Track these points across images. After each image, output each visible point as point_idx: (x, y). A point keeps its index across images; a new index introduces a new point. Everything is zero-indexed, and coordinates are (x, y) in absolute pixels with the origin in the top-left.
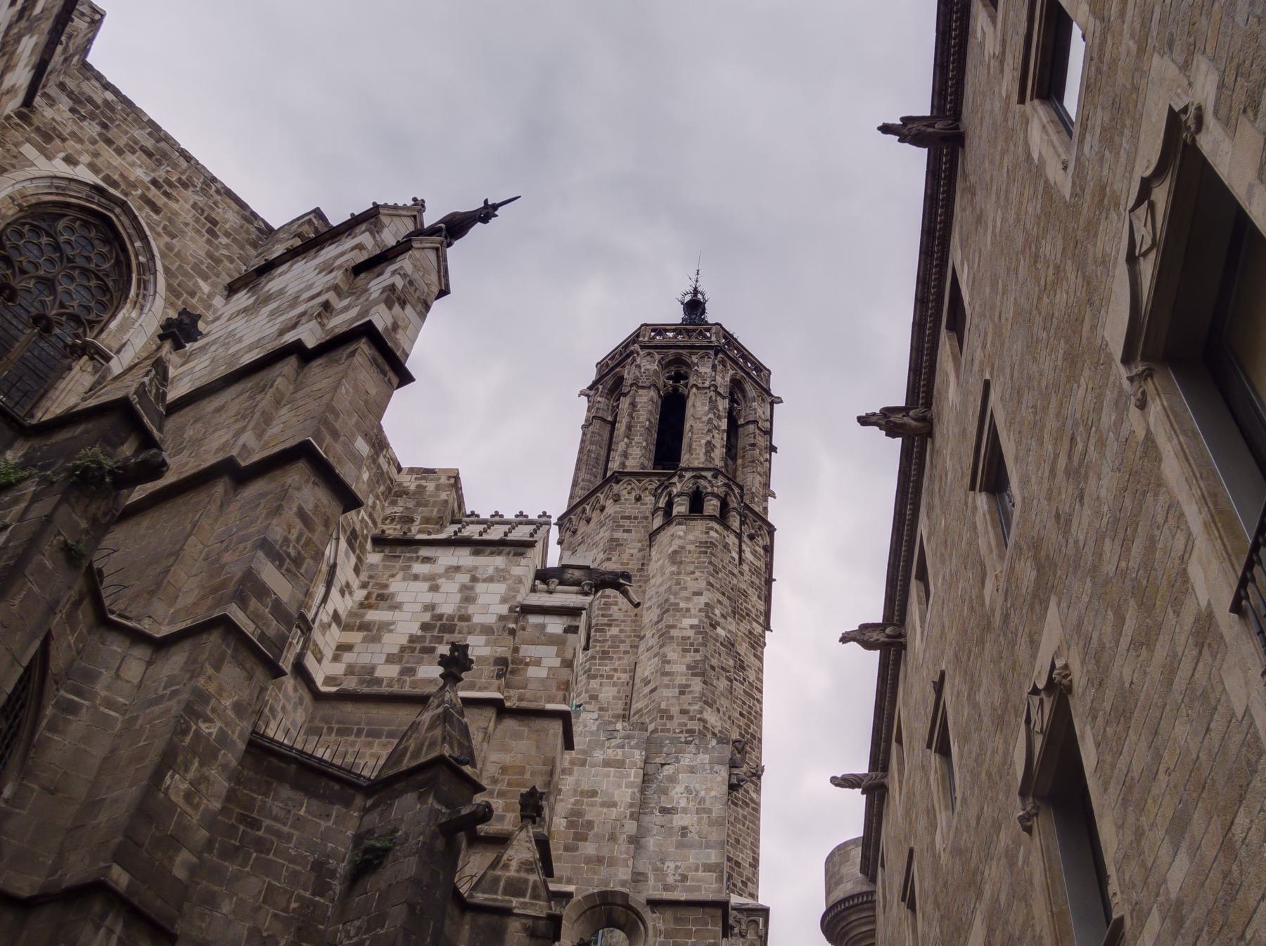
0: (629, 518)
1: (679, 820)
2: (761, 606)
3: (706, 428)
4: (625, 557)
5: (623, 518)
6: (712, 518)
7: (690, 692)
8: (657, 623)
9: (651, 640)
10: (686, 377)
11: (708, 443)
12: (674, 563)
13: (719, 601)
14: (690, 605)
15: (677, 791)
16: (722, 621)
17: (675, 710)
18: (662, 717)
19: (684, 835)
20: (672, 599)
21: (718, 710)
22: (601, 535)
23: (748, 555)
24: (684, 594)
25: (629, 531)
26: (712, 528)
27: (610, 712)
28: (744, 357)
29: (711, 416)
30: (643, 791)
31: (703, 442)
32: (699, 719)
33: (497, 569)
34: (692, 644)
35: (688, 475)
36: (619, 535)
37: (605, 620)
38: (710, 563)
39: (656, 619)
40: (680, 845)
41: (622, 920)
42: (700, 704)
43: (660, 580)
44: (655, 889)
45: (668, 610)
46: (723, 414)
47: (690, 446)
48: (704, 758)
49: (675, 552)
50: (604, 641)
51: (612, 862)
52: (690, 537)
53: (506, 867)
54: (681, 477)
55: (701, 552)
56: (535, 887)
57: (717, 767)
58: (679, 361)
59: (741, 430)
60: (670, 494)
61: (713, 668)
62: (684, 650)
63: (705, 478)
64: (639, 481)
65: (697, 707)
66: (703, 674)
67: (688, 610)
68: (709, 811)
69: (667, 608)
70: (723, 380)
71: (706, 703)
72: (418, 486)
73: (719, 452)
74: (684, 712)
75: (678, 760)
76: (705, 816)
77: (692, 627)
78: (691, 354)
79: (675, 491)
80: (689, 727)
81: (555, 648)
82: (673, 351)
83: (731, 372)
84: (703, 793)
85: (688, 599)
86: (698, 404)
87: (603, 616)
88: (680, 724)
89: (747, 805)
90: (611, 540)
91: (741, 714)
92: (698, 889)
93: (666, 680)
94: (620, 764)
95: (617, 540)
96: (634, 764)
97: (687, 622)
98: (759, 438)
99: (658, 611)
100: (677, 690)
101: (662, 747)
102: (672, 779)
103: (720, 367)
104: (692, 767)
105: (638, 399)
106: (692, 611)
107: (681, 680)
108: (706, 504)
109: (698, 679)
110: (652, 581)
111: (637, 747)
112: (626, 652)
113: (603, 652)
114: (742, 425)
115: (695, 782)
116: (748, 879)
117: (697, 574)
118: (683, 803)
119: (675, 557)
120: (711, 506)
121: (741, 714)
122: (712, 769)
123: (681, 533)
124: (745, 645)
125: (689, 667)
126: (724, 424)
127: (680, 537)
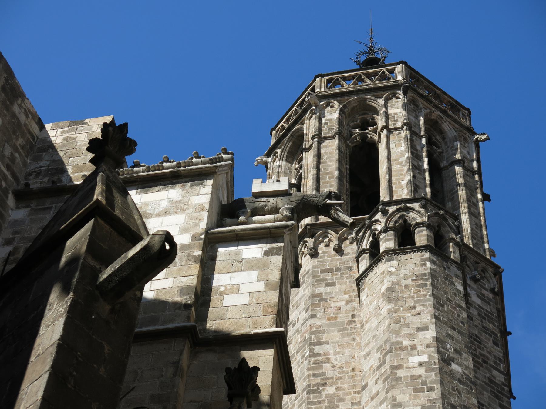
0: (330, 271)
2: (498, 352)
4: (331, 312)
5: (323, 271)
12: (390, 300)
13: (448, 336)
14: (416, 342)
16: (456, 356)
20: (394, 339)
22: (300, 295)
23: (475, 299)
24: (406, 331)
25: (332, 284)
28: (437, 97)
33: (171, 201)
34: (424, 383)
35: (391, 209)
36: (321, 289)
37: (318, 380)
39: (376, 364)
45: (390, 351)
49: (389, 290)
50: (319, 402)
52: (404, 272)
55: (418, 286)
62: (416, 390)
63: (413, 209)
67: (413, 347)
72: (65, 139)
77: (421, 364)
79: (379, 227)
81: (254, 274)
83: (424, 111)
85: (411, 337)
87: (314, 375)
90: (313, 296)
95: (320, 295)
99: (379, 355)
105: (322, 151)
106: (419, 348)
110: (367, 327)
114: (446, 168)
117: (419, 309)
119: (391, 295)
123: (393, 269)
127: (392, 273)
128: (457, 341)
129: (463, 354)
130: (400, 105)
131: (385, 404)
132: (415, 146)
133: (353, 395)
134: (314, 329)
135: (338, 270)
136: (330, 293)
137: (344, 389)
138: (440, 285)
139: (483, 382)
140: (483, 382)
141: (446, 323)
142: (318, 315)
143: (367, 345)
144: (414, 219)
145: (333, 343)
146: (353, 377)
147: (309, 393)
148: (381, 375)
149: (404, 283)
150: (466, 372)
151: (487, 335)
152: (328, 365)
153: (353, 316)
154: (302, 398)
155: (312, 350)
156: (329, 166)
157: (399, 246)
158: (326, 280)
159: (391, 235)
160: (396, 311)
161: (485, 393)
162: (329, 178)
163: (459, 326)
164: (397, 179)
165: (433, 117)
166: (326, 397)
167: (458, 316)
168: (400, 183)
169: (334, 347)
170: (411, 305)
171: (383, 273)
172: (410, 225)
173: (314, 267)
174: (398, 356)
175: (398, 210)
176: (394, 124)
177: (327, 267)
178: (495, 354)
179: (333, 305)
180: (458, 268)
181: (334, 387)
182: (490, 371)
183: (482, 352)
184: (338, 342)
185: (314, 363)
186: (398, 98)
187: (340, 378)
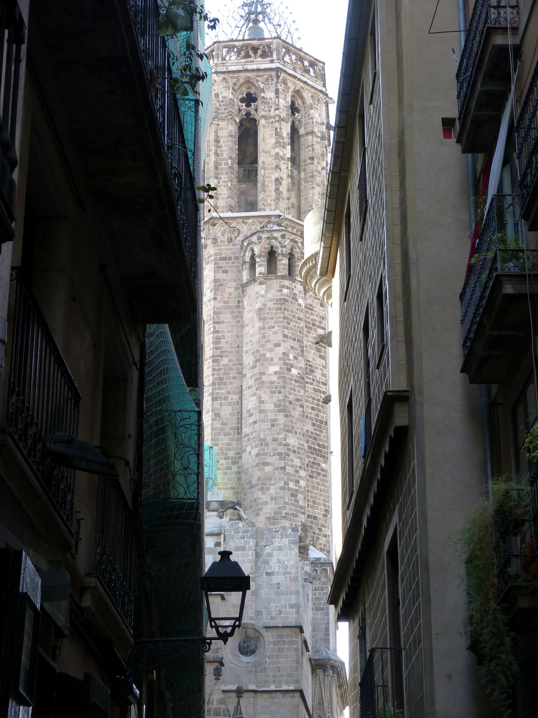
0: (224, 259)
1: (275, 579)
3: (274, 163)
5: (221, 259)
6: (283, 277)
7: (278, 425)
8: (254, 367)
9: (248, 382)
10: (255, 100)
11: (277, 180)
13: (292, 348)
14: (273, 356)
17: (269, 438)
18: (262, 444)
19: (278, 588)
21: (296, 433)
24: (269, 346)
25: (225, 272)
26: (283, 286)
29: (277, 150)
30: (256, 562)
31: (273, 177)
32: (284, 445)
34: (276, 387)
35: (264, 236)
36: (220, 276)
37: (218, 352)
38: (285, 318)
39: (251, 364)
40: (277, 594)
41: (252, 635)
43: (252, 331)
46: (287, 140)
47: (264, 185)
48: (286, 541)
49: (260, 309)
50: (219, 370)
52: (270, 296)
53: (212, 703)
54: (260, 238)
56: (224, 711)
57: (293, 546)
58: (248, 81)
59: (302, 139)
60: (253, 251)
61: (291, 403)
62: (272, 392)
63: (276, 239)
65: (282, 436)
66: (284, 411)
67: (272, 359)
68: (290, 573)
69: (260, 359)
70: (284, 102)
71: (288, 431)
73: (286, 183)
75: (272, 544)
76: (288, 576)
77: (275, 373)
80: (278, 451)
82: (243, 75)
83: (292, 88)
84: (286, 562)
85: (271, 350)
86: (267, 136)
87: (216, 348)
89: (319, 474)
90: (215, 281)
91: (313, 409)
96: (250, 548)
97: (273, 369)
98: (317, 147)
100: (269, 423)
101: (264, 535)
102: (270, 555)
104: (280, 547)
105: (220, 134)
106: (276, 360)
107: (271, 416)
108: (278, 263)
109: (282, 414)
111: (251, 537)
112: (234, 378)
113: (220, 379)
116: (323, 526)
117: (276, 329)
118: (277, 570)
120: (283, 263)
121: (313, 409)
122: (290, 547)
123: (263, 292)
124: (312, 351)
125: (276, 406)
126: (287, 152)
127: (262, 296)
128: (296, 349)
129: (299, 358)
130: (274, 89)
131: (255, 398)
132: (282, 134)
133: (238, 366)
134: (215, 310)
135: (230, 259)
136: (225, 280)
137: (232, 361)
138: (289, 306)
139: (312, 342)
140: (312, 342)
141: (291, 338)
142: (218, 298)
143: (247, 344)
144: (277, 248)
145: (227, 323)
146: (238, 352)
147: (213, 361)
148: (254, 375)
149: (270, 304)
150: (299, 372)
151: (317, 301)
152: (223, 341)
153: (239, 302)
154: (209, 363)
155: (214, 327)
156: (224, 151)
157: (268, 274)
158: (222, 267)
159: (263, 261)
160: (264, 328)
161: (312, 351)
162: (224, 165)
163: (298, 336)
164: (269, 173)
165: (297, 89)
166: (223, 366)
167: (298, 327)
168: (271, 177)
169: (227, 326)
171: (257, 293)
172: (275, 252)
173: (216, 254)
174: (263, 365)
175: (268, 238)
176: (270, 111)
177: (223, 256)
178: (321, 315)
179: (228, 290)
180: (301, 285)
181: (227, 359)
182: (316, 331)
183: (312, 317)
184: (230, 322)
185: (216, 339)
186: (273, 80)
187: (230, 352)
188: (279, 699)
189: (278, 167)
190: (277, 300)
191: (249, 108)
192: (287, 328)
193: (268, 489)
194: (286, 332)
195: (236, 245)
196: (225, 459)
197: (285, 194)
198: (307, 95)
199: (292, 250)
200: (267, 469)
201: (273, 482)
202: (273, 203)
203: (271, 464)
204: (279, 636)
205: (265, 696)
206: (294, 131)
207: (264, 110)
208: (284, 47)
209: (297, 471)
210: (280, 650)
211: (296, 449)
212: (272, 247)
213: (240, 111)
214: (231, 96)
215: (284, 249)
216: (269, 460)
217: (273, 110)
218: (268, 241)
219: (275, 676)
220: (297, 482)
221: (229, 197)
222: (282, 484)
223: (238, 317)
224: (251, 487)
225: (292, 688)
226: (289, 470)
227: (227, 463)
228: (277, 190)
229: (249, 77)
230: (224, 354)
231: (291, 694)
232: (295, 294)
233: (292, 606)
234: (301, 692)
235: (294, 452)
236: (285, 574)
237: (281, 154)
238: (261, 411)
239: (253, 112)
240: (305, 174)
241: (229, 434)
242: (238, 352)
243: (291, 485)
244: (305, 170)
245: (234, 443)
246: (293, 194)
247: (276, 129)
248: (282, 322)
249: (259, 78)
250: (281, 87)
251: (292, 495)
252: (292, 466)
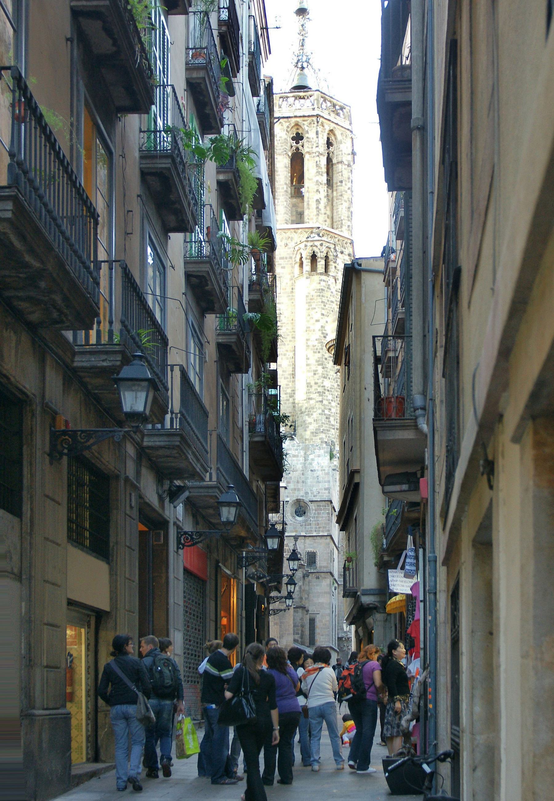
3: (316, 188)
6: (321, 274)
7: (318, 374)
10: (302, 138)
11: (317, 201)
15: (315, 464)
17: (312, 383)
21: (329, 378)
27: (287, 373)
34: (317, 349)
38: (322, 302)
42: (322, 379)
44: (311, 496)
46: (324, 170)
47: (308, 204)
48: (322, 451)
51: (299, 490)
57: (326, 454)
58: (297, 125)
61: (326, 359)
62: (314, 352)
63: (317, 246)
64: (285, 232)
68: (324, 470)
70: (323, 141)
71: (324, 377)
73: (324, 201)
74: (316, 383)
78: (304, 121)
82: (293, 120)
83: (327, 128)
88: (315, 389)
92: (323, 496)
93: (308, 367)
94: (297, 456)
100: (313, 373)
103: (320, 129)
107: (314, 368)
109: (321, 367)
111: (302, 449)
112: (290, 341)
115: (320, 460)
120: (321, 264)
125: (317, 361)
126: (324, 178)
135: (286, 258)
146: (292, 323)
153: (292, 289)
157: (311, 271)
160: (309, 309)
170: (315, 307)
175: (311, 246)
176: (312, 148)
177: (282, 256)
188: (319, 540)
189: (318, 191)
190: (317, 290)
191: (298, 145)
192: (323, 309)
193: (312, 415)
194: (324, 312)
195: (290, 248)
196: (285, 394)
197: (323, 211)
198: (338, 132)
199: (327, 254)
200: (312, 402)
201: (315, 410)
202: (315, 218)
203: (314, 399)
204: (318, 506)
205: (310, 538)
206: (329, 160)
207: (308, 147)
208: (322, 97)
209: (330, 403)
210: (318, 513)
211: (329, 389)
212: (314, 252)
213: (292, 147)
214: (286, 137)
215: (322, 254)
216: (312, 396)
217: (314, 147)
218: (311, 248)
219: (316, 528)
220: (330, 409)
221: (285, 213)
222: (320, 411)
223: (292, 299)
224: (302, 413)
225: (326, 534)
226: (325, 402)
227: (286, 397)
228: (317, 208)
229: (298, 122)
230: (283, 325)
231: (325, 538)
232: (329, 285)
233: (326, 489)
234: (331, 536)
235: (328, 391)
236: (321, 470)
237: (320, 181)
238: (307, 365)
239: (300, 148)
240: (337, 193)
241: (287, 378)
242: (292, 323)
243: (327, 412)
244: (337, 190)
245: (291, 384)
246: (328, 208)
247: (317, 162)
248: (319, 305)
249: (304, 122)
250: (320, 129)
251: (327, 418)
252: (327, 400)
